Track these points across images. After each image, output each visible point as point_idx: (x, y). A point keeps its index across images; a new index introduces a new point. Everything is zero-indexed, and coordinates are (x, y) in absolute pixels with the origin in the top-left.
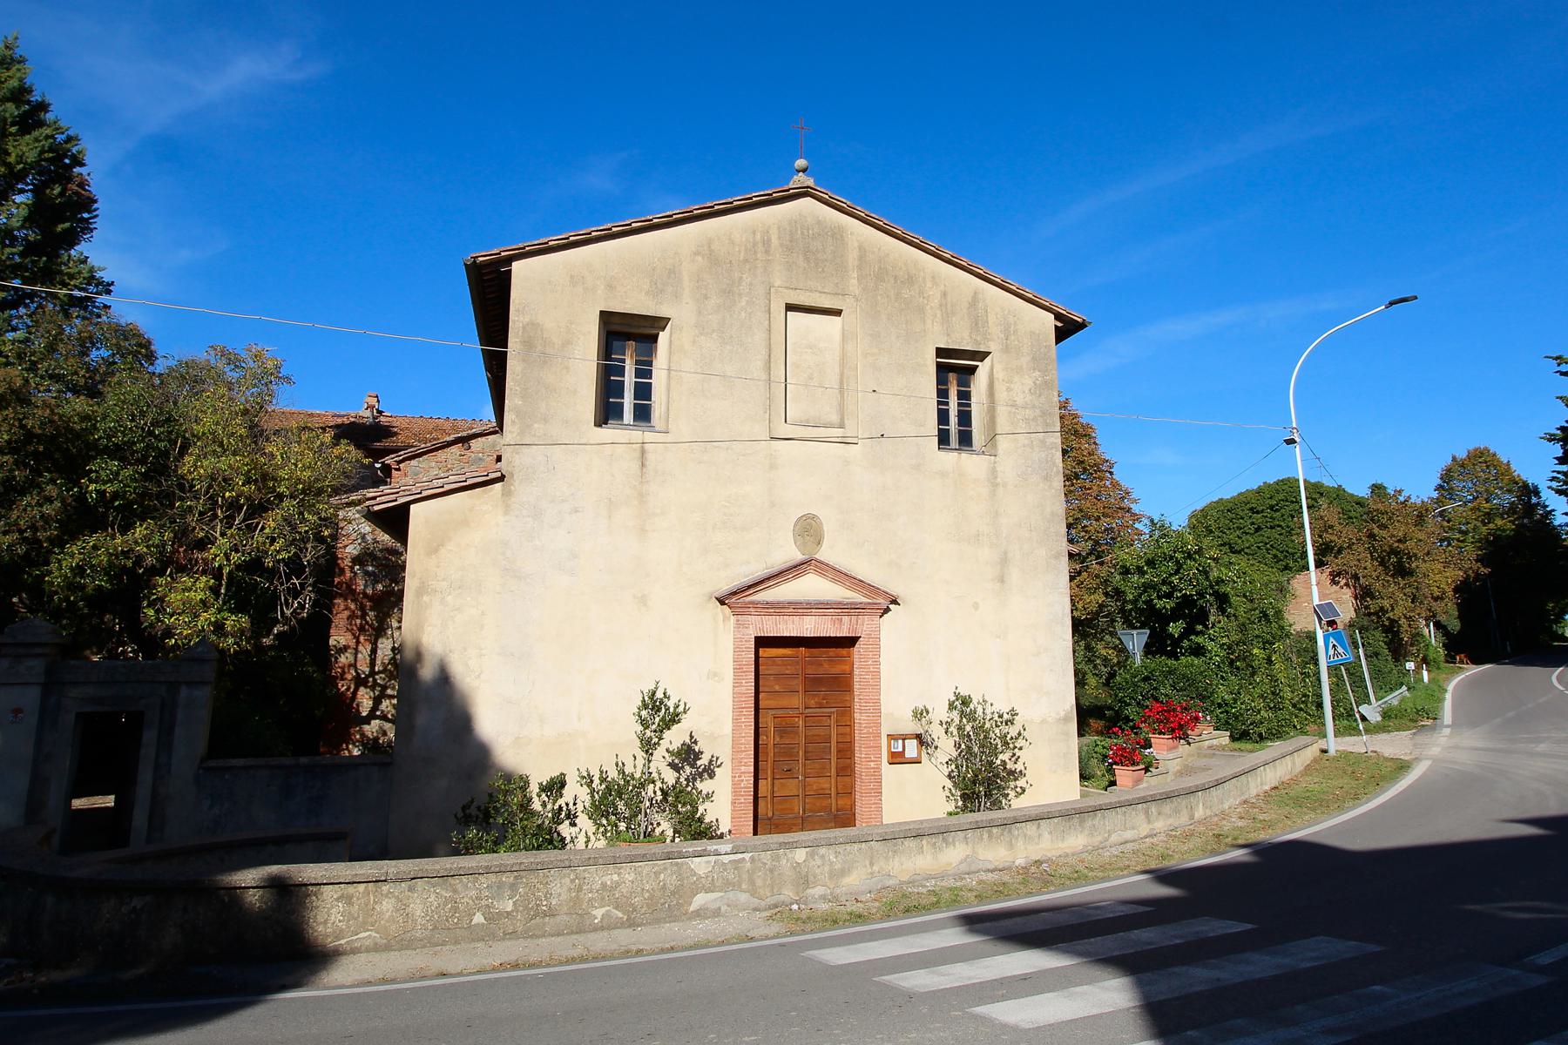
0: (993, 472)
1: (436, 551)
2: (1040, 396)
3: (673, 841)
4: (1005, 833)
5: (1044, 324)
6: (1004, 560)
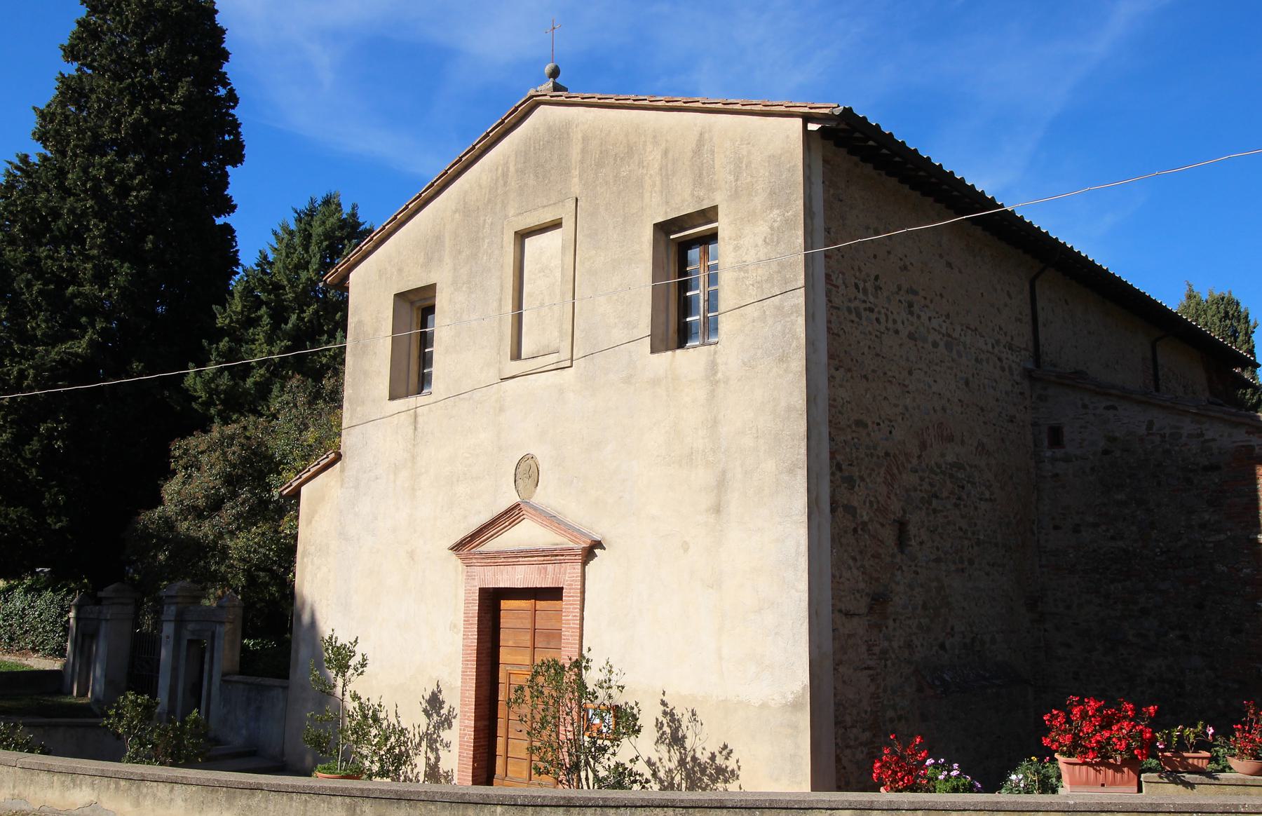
0: (713, 367)
1: (311, 522)
2: (778, 242)
3: (424, 782)
4: (133, 788)
5: (788, 137)
6: (721, 484)
